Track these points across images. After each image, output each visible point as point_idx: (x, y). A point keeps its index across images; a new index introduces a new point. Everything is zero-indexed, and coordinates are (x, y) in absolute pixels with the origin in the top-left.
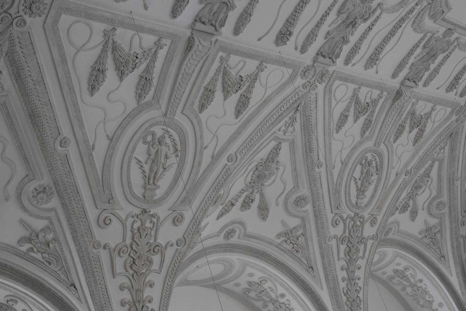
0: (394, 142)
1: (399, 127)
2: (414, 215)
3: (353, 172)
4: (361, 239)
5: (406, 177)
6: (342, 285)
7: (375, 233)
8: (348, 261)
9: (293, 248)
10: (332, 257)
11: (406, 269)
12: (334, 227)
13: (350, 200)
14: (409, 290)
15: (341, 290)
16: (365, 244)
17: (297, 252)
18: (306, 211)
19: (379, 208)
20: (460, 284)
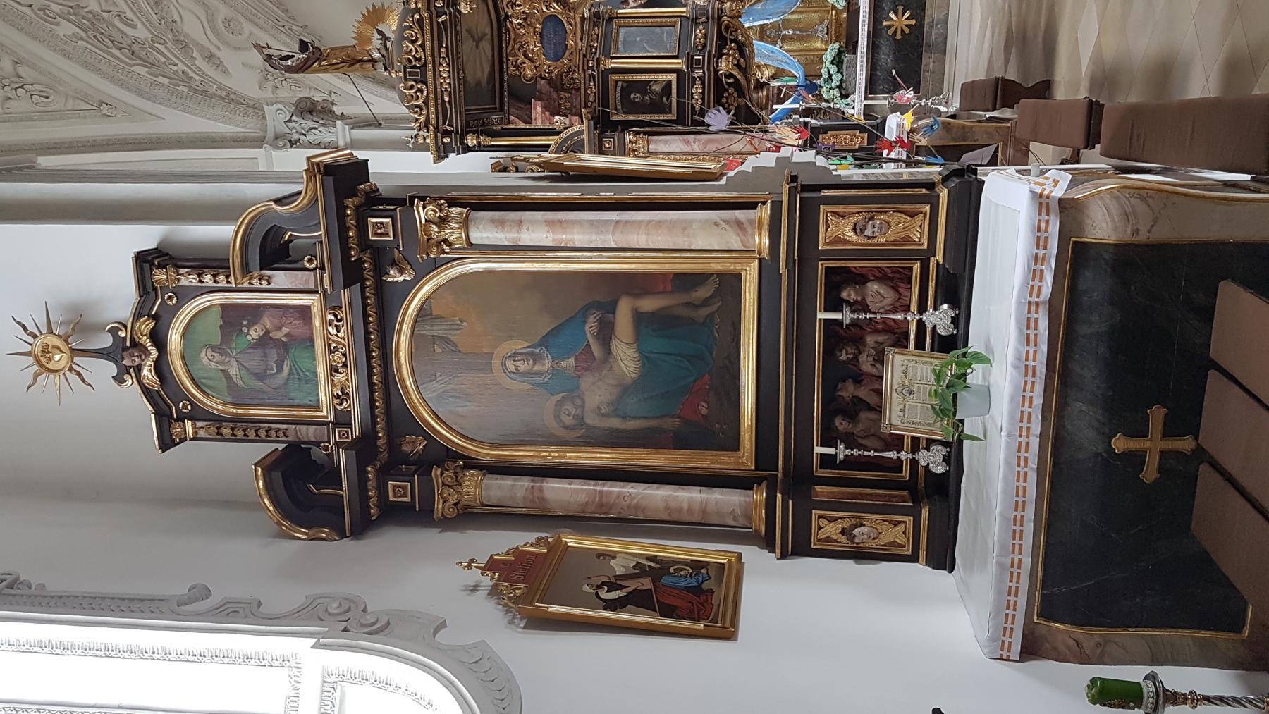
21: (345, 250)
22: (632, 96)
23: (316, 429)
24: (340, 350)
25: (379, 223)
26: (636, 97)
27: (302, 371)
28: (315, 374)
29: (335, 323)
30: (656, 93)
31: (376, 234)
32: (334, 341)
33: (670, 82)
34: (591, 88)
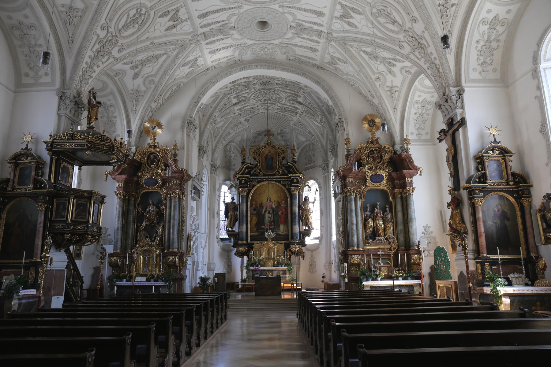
0: (159, 18)
1: (167, 11)
2: (136, 76)
3: (131, 10)
4: (109, 52)
5: (150, 45)
6: (84, 65)
7: (117, 57)
8: (95, 56)
9: (69, 20)
10: (89, 44)
11: (111, 105)
12: (102, 30)
13: (119, 24)
14: (105, 119)
15: (82, 67)
16: (109, 57)
17: (70, 24)
18: (92, 4)
19: (128, 46)
20: (135, 130)
26: (61, 207)
33: (64, 217)
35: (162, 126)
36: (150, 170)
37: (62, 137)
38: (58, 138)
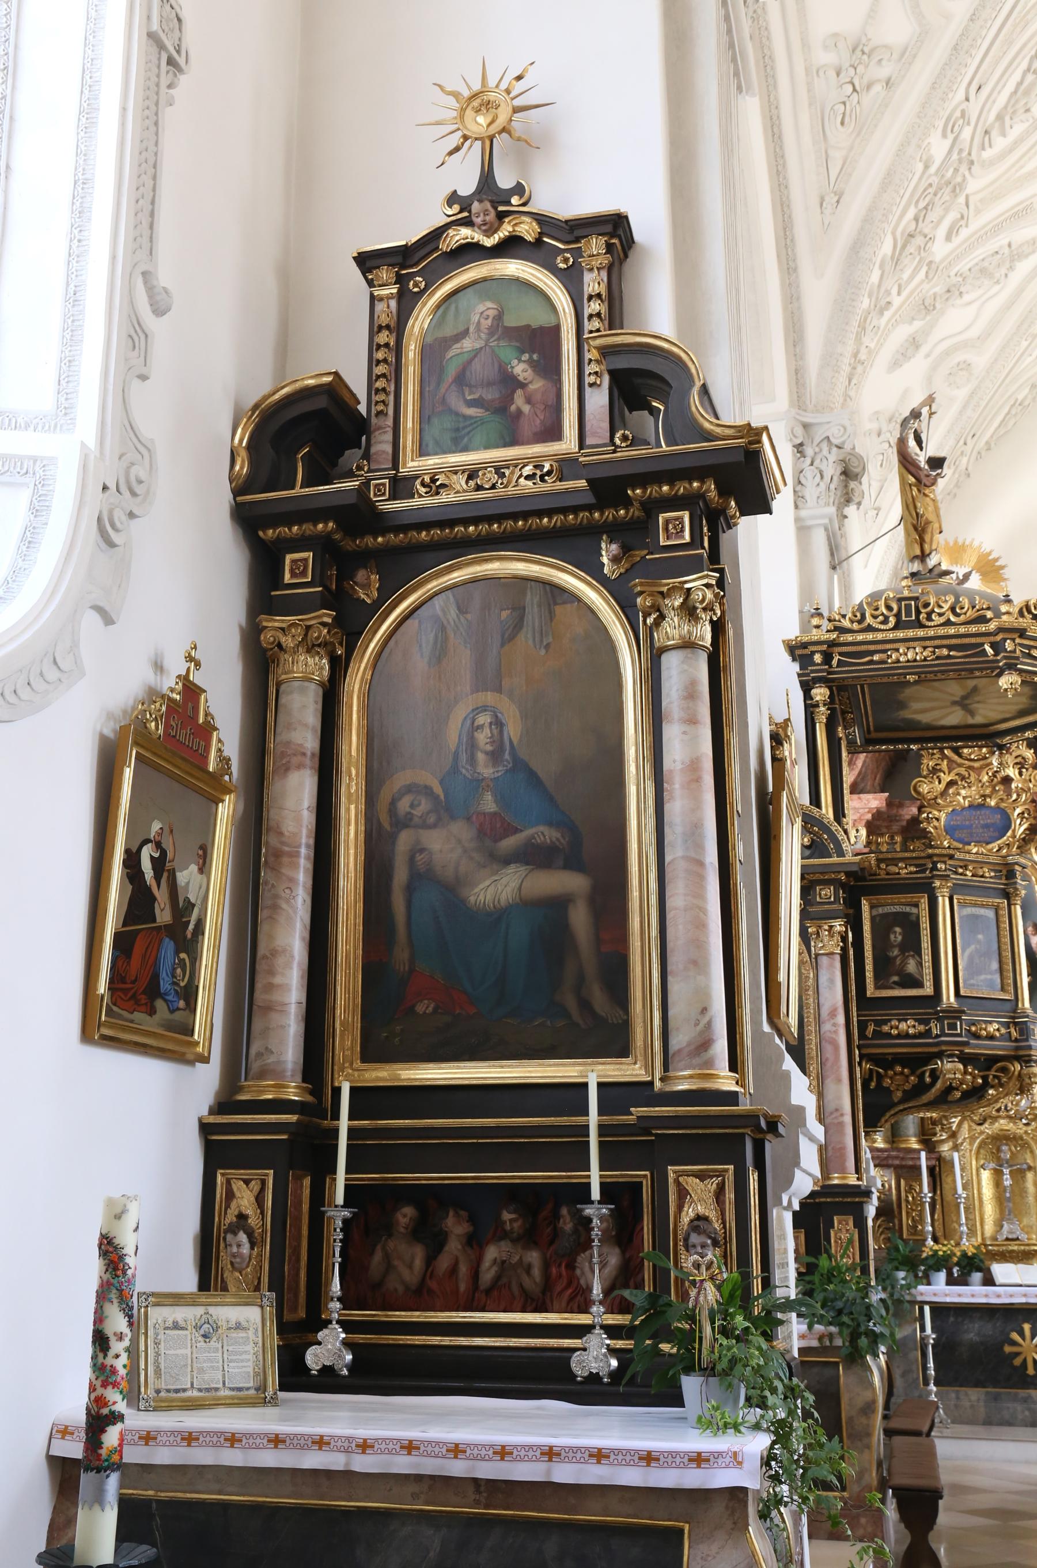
21: (644, 479)
22: (898, 930)
23: (387, 453)
24: (500, 481)
25: (683, 527)
26: (897, 935)
27: (469, 433)
28: (465, 449)
29: (539, 473)
30: (904, 963)
31: (667, 522)
32: (512, 473)
33: (919, 984)
34: (906, 868)
35: (1002, 567)
36: (962, 771)
37: (869, 620)
38: (846, 623)
